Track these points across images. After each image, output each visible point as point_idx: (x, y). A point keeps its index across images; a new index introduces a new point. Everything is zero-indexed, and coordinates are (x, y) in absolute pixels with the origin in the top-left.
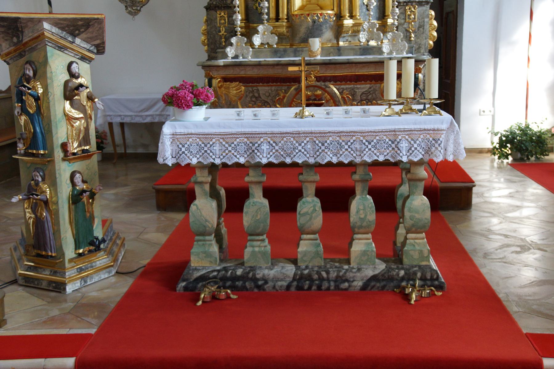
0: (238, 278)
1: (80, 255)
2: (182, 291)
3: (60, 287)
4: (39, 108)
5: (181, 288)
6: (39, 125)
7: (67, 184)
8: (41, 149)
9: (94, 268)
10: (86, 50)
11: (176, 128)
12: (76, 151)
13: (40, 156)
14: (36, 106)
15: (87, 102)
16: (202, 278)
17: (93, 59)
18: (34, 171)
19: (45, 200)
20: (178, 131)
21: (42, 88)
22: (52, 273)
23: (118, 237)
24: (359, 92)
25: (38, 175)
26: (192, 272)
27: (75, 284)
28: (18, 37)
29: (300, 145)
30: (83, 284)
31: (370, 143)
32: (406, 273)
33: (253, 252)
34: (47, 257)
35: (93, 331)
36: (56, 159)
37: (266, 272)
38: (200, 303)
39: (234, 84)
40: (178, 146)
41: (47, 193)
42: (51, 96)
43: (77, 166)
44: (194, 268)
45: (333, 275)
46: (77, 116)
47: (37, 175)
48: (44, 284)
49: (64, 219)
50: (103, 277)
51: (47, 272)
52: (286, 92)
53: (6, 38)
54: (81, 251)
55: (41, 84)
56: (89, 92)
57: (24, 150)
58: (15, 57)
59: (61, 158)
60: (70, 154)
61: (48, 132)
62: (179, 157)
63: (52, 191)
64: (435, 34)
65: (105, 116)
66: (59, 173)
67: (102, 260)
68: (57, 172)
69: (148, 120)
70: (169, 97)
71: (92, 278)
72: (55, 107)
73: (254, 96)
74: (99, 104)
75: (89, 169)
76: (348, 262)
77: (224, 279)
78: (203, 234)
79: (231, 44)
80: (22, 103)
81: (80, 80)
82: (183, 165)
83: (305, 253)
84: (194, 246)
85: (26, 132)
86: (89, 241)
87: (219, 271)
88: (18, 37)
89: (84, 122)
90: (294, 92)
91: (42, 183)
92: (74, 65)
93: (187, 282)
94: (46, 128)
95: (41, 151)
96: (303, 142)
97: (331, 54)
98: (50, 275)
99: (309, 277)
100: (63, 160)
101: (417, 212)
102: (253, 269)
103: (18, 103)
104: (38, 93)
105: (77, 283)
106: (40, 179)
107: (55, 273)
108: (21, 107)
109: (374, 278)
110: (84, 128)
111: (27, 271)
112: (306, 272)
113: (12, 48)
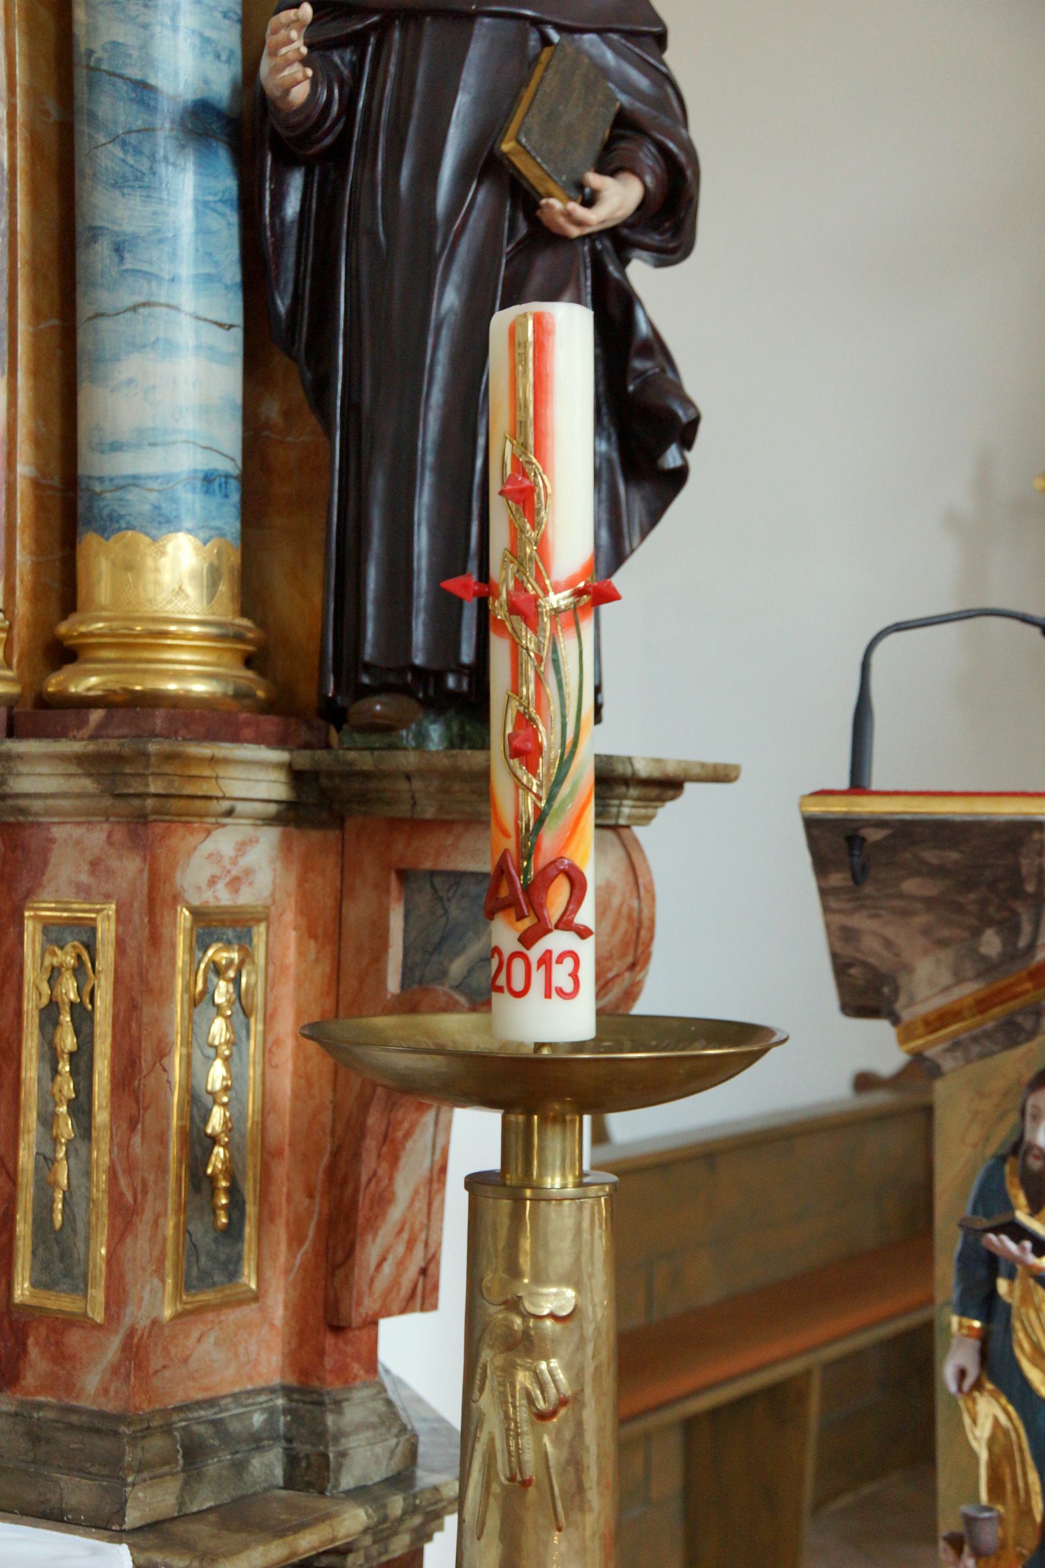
28: (1010, 929)
53: (945, 933)
58: (975, 1039)
80: (987, 1317)
85: (1000, 1508)
88: (1010, 929)
103: (963, 1313)
108: (985, 1339)
113: (970, 989)
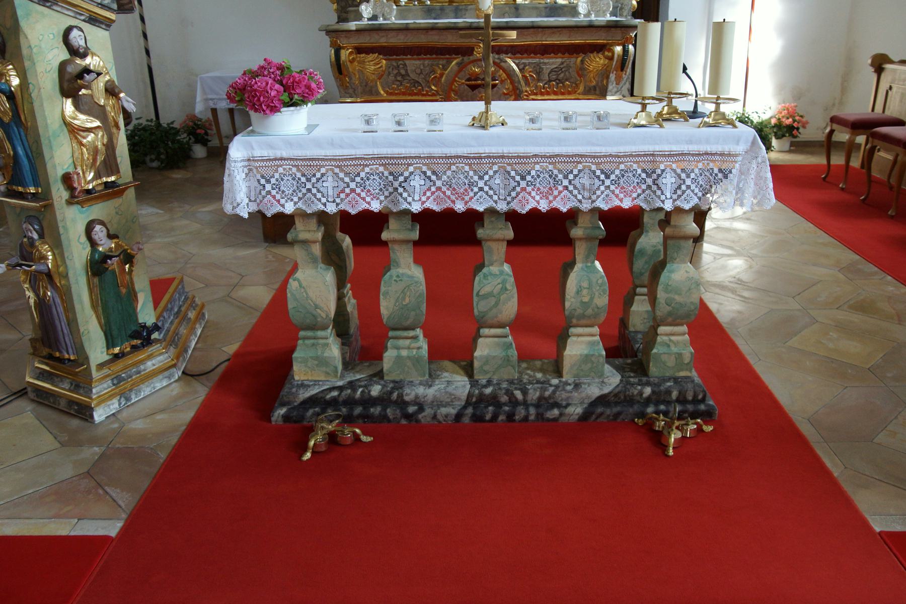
0: (374, 401)
1: (116, 357)
2: (280, 422)
3: (84, 412)
5: (278, 417)
6: (21, 143)
7: (81, 243)
8: (28, 184)
9: (143, 373)
10: (96, 4)
11: (252, 148)
12: (91, 187)
13: (30, 197)
14: (11, 109)
15: (107, 99)
16: (312, 401)
17: (113, 21)
18: (25, 222)
19: (47, 271)
20: (258, 153)
21: (18, 76)
22: (72, 388)
23: (193, 305)
24: (546, 69)
25: (32, 228)
26: (297, 391)
27: (109, 405)
29: (481, 178)
30: (123, 403)
31: (607, 177)
32: (653, 392)
33: (399, 358)
34: (61, 360)
35: (112, 528)
36: (55, 203)
37: (421, 390)
38: (308, 455)
39: (371, 57)
40: (259, 181)
41: (49, 259)
42: (33, 90)
43: (97, 211)
44: (300, 383)
45: (534, 395)
46: (89, 125)
47: (29, 229)
48: (63, 404)
49: (81, 302)
50: (158, 386)
51: (67, 386)
52: (445, 68)
54: (117, 350)
55: (15, 68)
56: (107, 82)
57: (5, 186)
59: (64, 201)
60: (79, 193)
61: (36, 156)
62: (261, 202)
63: (57, 256)
65: (206, 100)
66: (63, 227)
68: (60, 225)
70: (238, 91)
71: (140, 392)
72: (44, 111)
73: (399, 74)
74: (128, 101)
75: (120, 213)
76: (559, 373)
77: (350, 402)
78: (313, 327)
81: (88, 60)
82: (269, 215)
83: (487, 360)
84: (298, 348)
86: (130, 332)
87: (341, 389)
89: (103, 136)
90: (456, 68)
91: (40, 242)
92: (75, 33)
93: (289, 407)
94: (34, 149)
95: (30, 188)
96: (487, 173)
97: (506, 15)
98: (69, 390)
99: (493, 400)
100: (69, 203)
101: (678, 291)
102: (398, 385)
104: (10, 86)
105: (113, 404)
106: (35, 236)
107: (76, 387)
109: (602, 400)
110: (104, 145)
111: (38, 379)
112: (488, 391)
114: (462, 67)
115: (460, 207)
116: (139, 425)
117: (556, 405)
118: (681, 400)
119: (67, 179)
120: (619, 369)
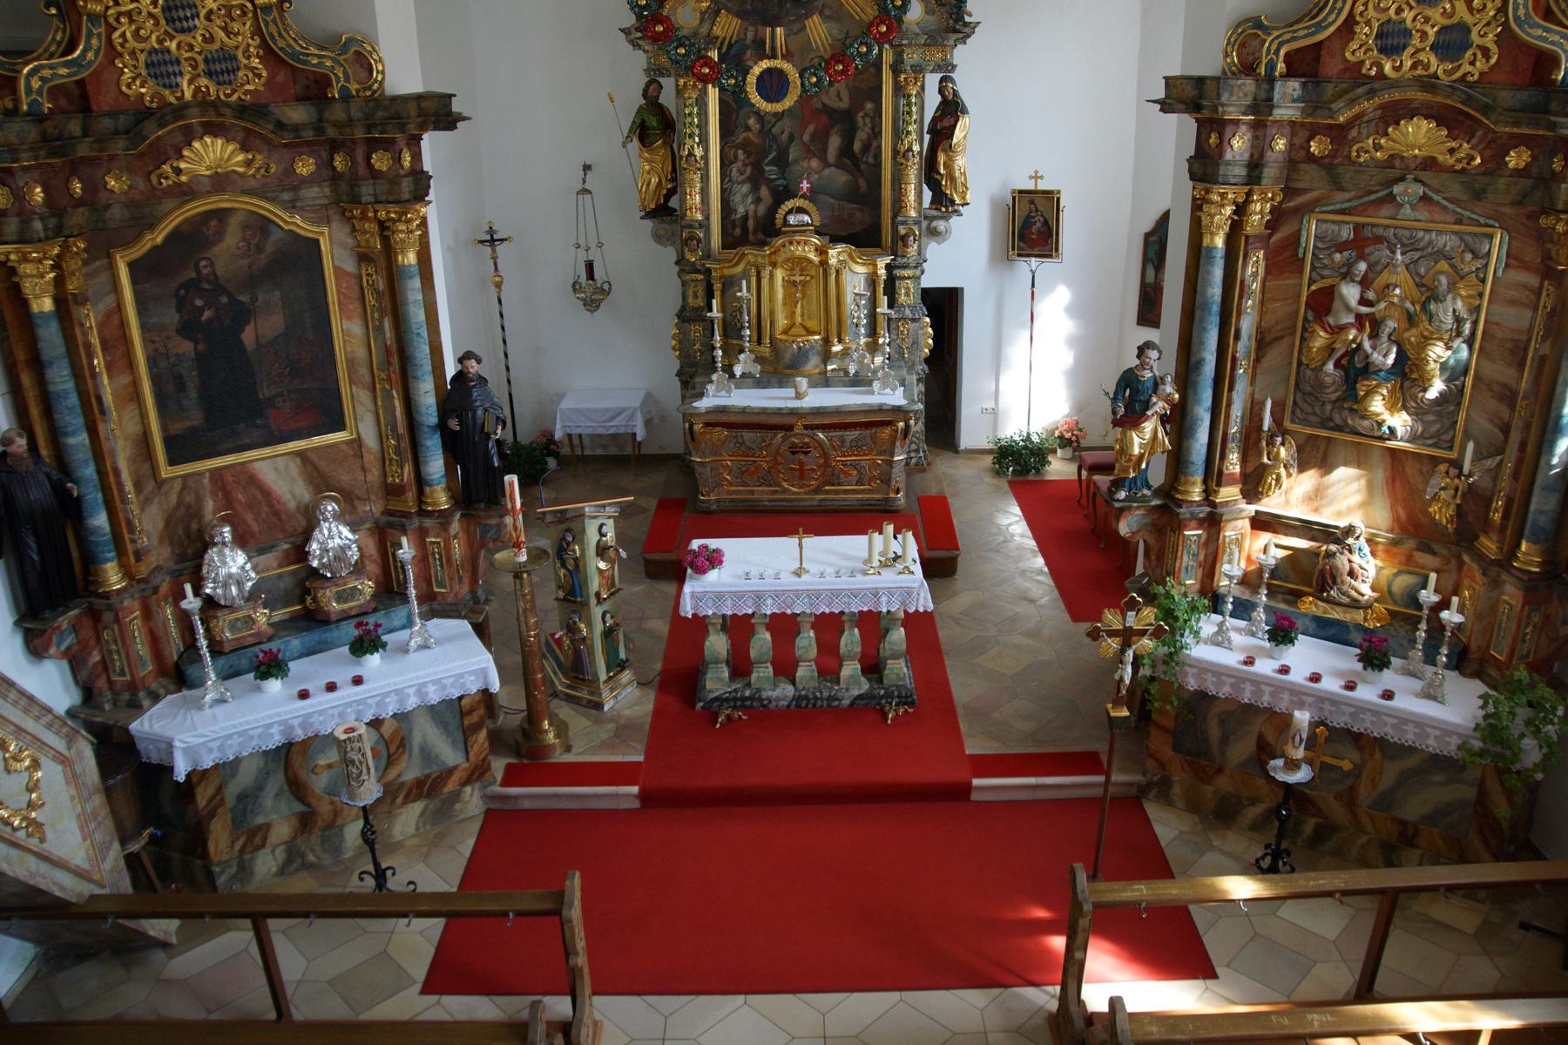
3: (598, 706)
4: (577, 566)
16: (716, 699)
20: (697, 590)
24: (849, 439)
35: (641, 758)
37: (770, 693)
39: (717, 429)
43: (606, 606)
45: (826, 694)
48: (584, 702)
52: (772, 439)
61: (584, 583)
64: (931, 341)
65: (564, 427)
67: (626, 676)
69: (612, 431)
76: (838, 683)
77: (735, 699)
78: (717, 663)
79: (711, 382)
99: (806, 697)
102: (758, 690)
107: (592, 694)
109: (860, 697)
114: (784, 439)
115: (789, 612)
116: (627, 712)
117: (837, 699)
118: (899, 696)
119: (598, 595)
120: (869, 680)
